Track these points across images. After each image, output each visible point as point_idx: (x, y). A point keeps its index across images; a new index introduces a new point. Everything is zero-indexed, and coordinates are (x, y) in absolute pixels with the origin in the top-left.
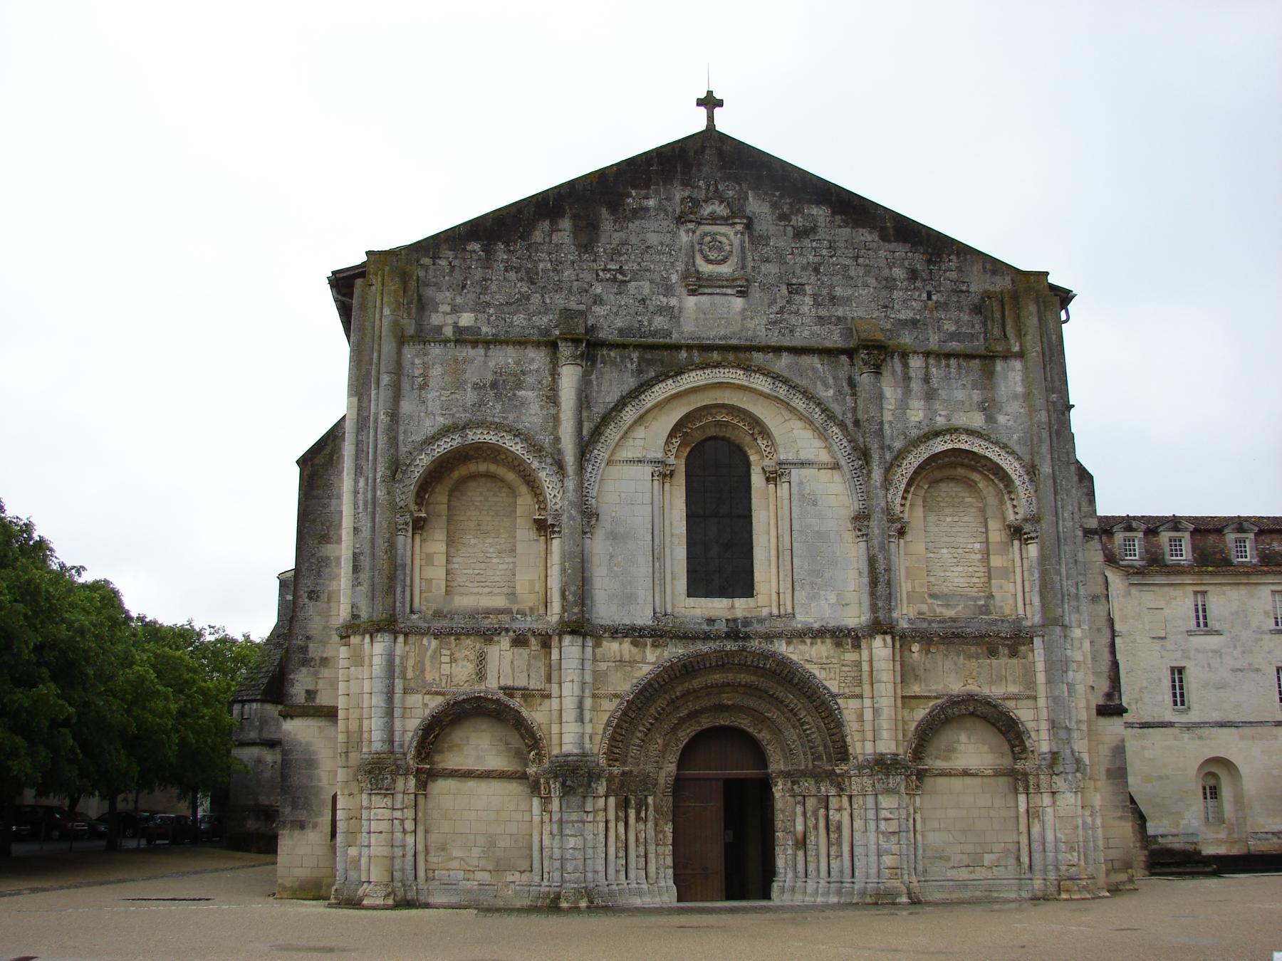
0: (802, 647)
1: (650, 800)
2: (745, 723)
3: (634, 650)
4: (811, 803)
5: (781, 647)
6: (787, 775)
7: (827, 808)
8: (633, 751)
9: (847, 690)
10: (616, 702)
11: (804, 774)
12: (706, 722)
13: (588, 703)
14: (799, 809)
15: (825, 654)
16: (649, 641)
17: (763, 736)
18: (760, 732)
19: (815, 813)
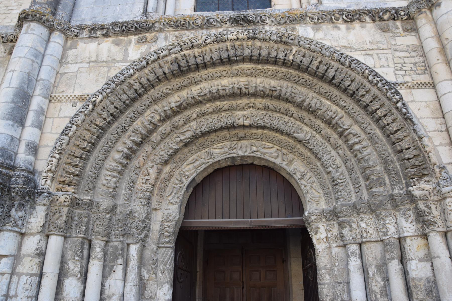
0: (335, 33)
1: (134, 250)
2: (268, 152)
3: (115, 49)
4: (373, 252)
5: (305, 31)
6: (333, 215)
7: (403, 260)
8: (107, 178)
9: (407, 79)
10: (80, 105)
11: (356, 209)
12: (221, 151)
13: (37, 102)
14: (354, 264)
15: (368, 39)
16: (134, 38)
17: (294, 167)
18: (290, 162)
19: (383, 268)
